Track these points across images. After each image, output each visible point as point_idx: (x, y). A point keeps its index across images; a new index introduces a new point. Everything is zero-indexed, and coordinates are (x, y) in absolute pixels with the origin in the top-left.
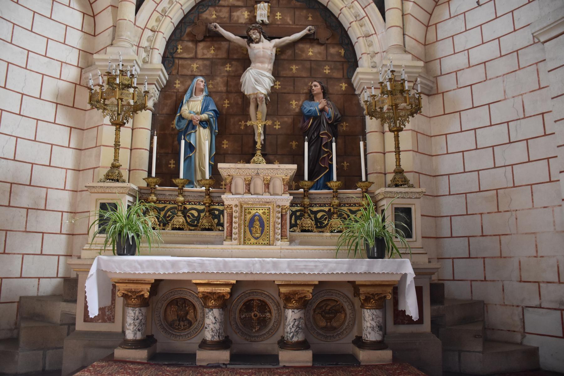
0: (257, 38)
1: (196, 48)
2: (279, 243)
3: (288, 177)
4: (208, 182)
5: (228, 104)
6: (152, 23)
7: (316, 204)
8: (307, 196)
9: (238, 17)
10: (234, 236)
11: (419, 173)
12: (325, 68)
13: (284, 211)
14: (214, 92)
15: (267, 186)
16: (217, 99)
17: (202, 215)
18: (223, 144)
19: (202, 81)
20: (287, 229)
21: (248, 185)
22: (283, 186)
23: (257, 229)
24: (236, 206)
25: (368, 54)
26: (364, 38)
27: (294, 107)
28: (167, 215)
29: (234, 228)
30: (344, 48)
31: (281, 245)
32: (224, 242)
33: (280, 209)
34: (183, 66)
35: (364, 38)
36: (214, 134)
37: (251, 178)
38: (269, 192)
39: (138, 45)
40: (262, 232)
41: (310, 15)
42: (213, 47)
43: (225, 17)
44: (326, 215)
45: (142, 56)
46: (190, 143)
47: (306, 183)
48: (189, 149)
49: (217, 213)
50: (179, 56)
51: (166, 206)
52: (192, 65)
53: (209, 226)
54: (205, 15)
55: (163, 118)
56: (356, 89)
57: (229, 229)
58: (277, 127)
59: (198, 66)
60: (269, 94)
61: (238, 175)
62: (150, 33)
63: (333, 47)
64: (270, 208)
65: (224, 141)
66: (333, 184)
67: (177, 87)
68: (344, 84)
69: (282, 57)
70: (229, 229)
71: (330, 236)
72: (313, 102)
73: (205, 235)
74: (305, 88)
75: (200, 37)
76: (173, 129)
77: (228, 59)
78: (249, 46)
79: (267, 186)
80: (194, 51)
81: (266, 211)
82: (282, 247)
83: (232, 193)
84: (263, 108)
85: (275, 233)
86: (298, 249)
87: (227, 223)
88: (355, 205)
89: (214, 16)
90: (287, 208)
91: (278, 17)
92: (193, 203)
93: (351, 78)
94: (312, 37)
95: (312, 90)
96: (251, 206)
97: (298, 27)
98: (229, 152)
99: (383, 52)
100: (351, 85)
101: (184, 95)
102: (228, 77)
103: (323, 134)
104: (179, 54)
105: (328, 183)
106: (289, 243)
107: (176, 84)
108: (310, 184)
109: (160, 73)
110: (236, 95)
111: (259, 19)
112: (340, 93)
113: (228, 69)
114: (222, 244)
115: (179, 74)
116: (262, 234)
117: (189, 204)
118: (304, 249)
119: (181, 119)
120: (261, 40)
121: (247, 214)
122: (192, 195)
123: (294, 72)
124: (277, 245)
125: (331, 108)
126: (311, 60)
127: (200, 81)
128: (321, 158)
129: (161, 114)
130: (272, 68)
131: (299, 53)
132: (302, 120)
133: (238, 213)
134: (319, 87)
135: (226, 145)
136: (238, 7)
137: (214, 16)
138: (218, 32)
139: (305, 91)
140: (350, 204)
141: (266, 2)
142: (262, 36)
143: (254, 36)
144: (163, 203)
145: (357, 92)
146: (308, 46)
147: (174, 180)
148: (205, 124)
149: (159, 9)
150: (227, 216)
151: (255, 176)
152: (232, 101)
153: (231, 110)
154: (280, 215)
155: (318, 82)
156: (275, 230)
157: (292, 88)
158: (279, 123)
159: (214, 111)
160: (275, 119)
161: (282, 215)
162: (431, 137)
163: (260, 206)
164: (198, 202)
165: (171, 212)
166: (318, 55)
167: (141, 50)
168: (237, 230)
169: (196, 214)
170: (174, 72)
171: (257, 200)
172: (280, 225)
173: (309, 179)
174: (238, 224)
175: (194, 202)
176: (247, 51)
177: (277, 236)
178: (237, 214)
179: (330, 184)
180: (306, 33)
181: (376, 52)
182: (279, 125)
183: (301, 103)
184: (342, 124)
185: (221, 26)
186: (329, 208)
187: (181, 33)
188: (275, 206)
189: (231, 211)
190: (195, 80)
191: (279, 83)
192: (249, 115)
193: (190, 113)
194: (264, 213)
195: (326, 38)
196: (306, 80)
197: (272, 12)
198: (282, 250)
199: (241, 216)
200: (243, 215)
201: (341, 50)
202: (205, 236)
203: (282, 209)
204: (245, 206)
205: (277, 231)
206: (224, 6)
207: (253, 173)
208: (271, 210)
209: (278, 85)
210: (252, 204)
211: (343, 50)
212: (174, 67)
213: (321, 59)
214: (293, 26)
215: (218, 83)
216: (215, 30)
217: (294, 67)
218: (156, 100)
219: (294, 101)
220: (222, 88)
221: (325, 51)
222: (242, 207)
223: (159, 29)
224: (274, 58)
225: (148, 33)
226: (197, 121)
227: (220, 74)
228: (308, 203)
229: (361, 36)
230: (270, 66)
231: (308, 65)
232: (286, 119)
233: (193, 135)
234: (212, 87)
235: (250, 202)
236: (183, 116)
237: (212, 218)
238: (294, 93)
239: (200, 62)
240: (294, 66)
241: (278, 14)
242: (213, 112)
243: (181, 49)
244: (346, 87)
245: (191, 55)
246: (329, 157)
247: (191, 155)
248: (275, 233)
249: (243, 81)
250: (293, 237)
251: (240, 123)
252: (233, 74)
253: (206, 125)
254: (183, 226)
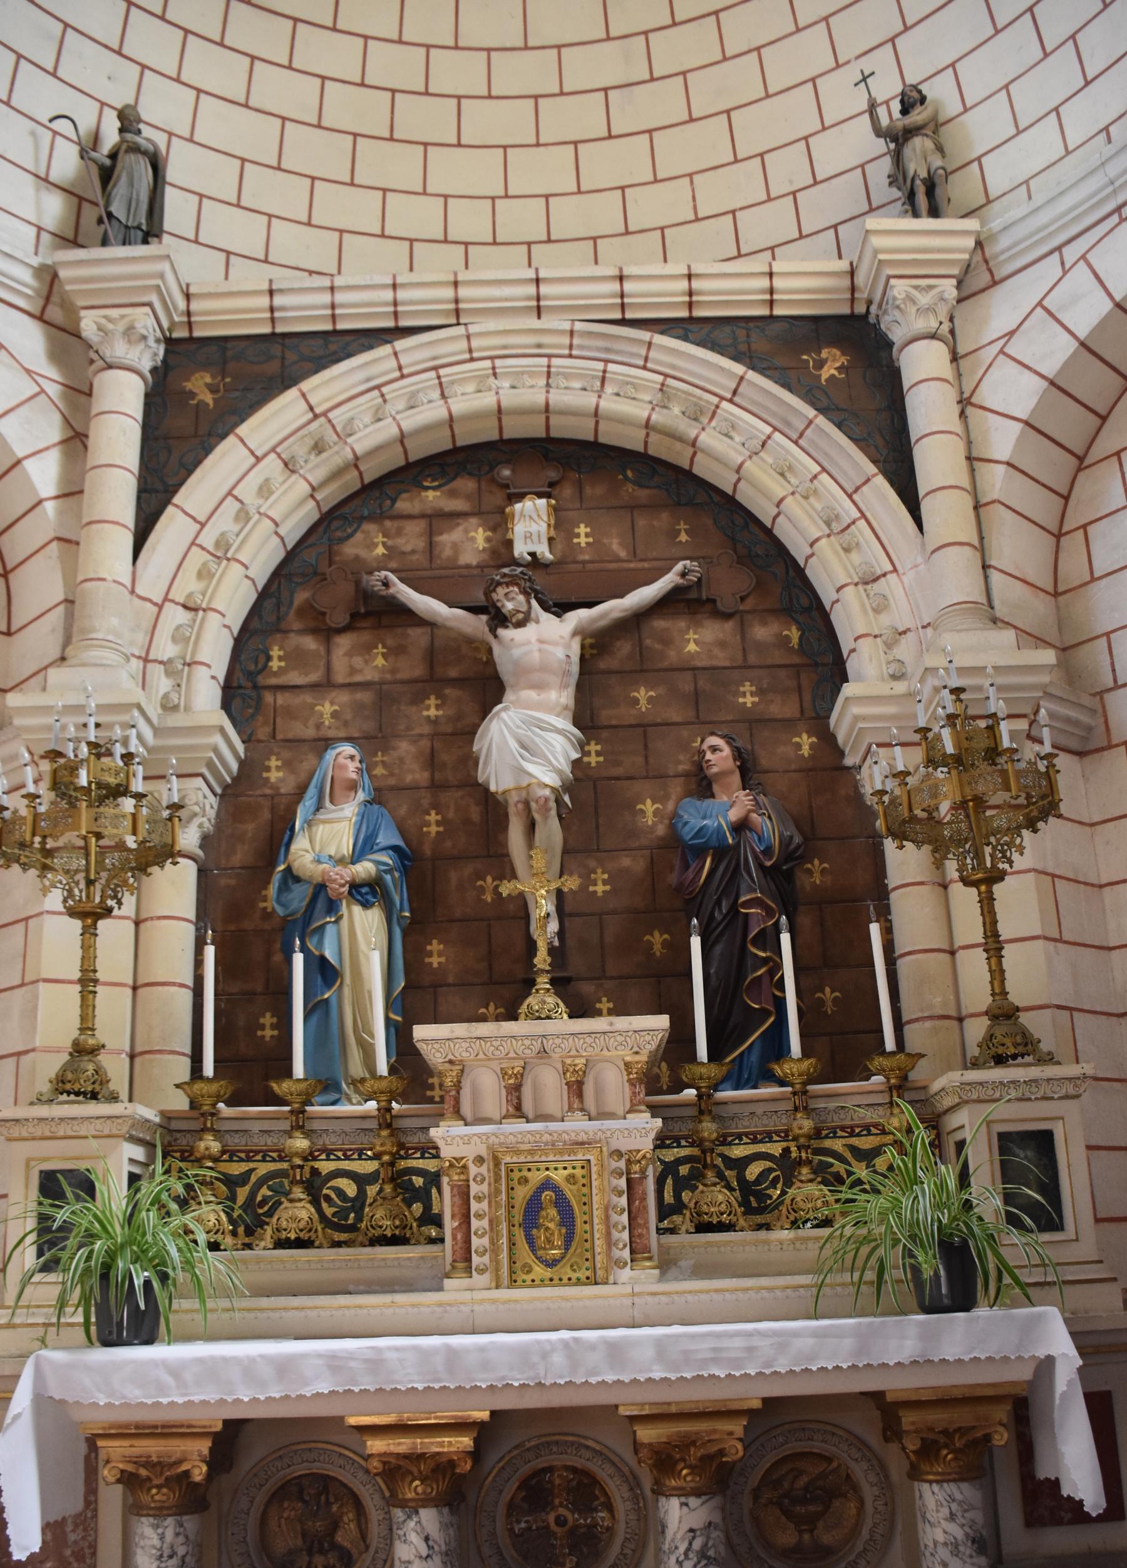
0: (519, 611)
1: (328, 652)
2: (626, 1274)
3: (643, 1058)
4: (384, 1085)
5: (438, 823)
6: (188, 585)
7: (739, 1136)
8: (710, 1112)
9: (455, 546)
10: (475, 1259)
11: (1071, 1009)
12: (742, 689)
13: (636, 1168)
14: (392, 788)
15: (576, 1089)
16: (403, 811)
17: (372, 1190)
18: (430, 954)
19: (352, 757)
20: (648, 1228)
21: (515, 1091)
22: (627, 1085)
23: (552, 1234)
24: (480, 1160)
25: (876, 636)
26: (860, 587)
27: (650, 823)
28: (259, 1198)
29: (476, 1234)
30: (797, 622)
31: (634, 1281)
32: (447, 1283)
33: (622, 1164)
34: (290, 713)
35: (860, 587)
36: (399, 924)
37: (524, 1068)
38: (582, 1110)
39: (143, 655)
40: (569, 1240)
41: (682, 526)
42: (380, 646)
43: (413, 552)
44: (775, 1170)
45: (157, 691)
46: (323, 959)
47: (703, 1070)
48: (319, 979)
49: (418, 1181)
50: (274, 681)
51: (254, 1170)
52: (318, 708)
53: (396, 1227)
54: (351, 549)
55: (233, 882)
56: (847, 752)
57: (459, 1237)
58: (600, 888)
59: (337, 708)
60: (567, 787)
61: (480, 1060)
62: (182, 616)
63: (764, 623)
64: (589, 1161)
65: (431, 944)
66: (791, 1069)
67: (273, 780)
68: (805, 736)
69: (603, 665)
70: (459, 1237)
71: (792, 1242)
72: (711, 800)
73: (384, 1259)
74: (682, 757)
75: (340, 618)
76: (267, 915)
78: (496, 636)
79: (576, 1089)
80: (322, 663)
81: (579, 1172)
82: (637, 1289)
83: (463, 1119)
84: (551, 831)
85: (610, 1243)
86: (690, 1292)
87: (453, 1217)
88: (869, 1131)
89: (380, 550)
90: (644, 1157)
91: (583, 540)
92: (340, 1154)
93: (829, 717)
94: (693, 595)
95: (705, 765)
96: (529, 1159)
97: (646, 565)
98: (451, 980)
99: (924, 627)
100: (827, 739)
101: (298, 802)
102: (433, 736)
103: (748, 904)
104: (275, 674)
105: (776, 1067)
106: (656, 1272)
107: (268, 769)
108: (715, 1071)
109: (218, 740)
110: (460, 793)
111: (521, 549)
112: (793, 767)
113: (433, 712)
114: (440, 1289)
115: (279, 736)
116: (567, 1249)
117: (328, 1159)
118: (708, 1292)
119: (290, 882)
120: (533, 615)
121: (515, 1184)
122: (337, 1129)
123: (644, 709)
124: (620, 1281)
125: (770, 818)
126: (694, 669)
128: (748, 980)
129: (225, 869)
130: (571, 703)
131: (657, 646)
132: (677, 863)
133: (486, 1183)
134: (727, 751)
135: (439, 956)
136: (454, 516)
137: (380, 550)
138: (393, 597)
139: (681, 768)
140: (852, 1128)
141: (540, 495)
142: (534, 603)
143: (509, 606)
144: (242, 1160)
145: (849, 761)
146: (682, 624)
147: (274, 1085)
148: (366, 894)
149: (208, 538)
150: (453, 1196)
151: (535, 1061)
152: (451, 815)
153: (448, 844)
154: (622, 1183)
155: (723, 737)
156: (608, 1234)
157: (640, 760)
158: (606, 876)
159: (395, 848)
160: (592, 863)
161: (629, 1181)
162: (1101, 886)
163: (558, 1158)
164: (357, 1149)
165: (269, 1188)
166: (716, 651)
167: (155, 671)
168: (485, 1241)
169: (351, 1189)
170: (263, 732)
171: (546, 1138)
172: (625, 1216)
173: (715, 1054)
174: (487, 1219)
175: (345, 1151)
176: (490, 651)
177: (616, 1253)
178: (485, 1188)
179: (782, 1070)
180: (673, 585)
181: (901, 629)
182: (605, 883)
183: (670, 806)
184: (809, 866)
185: (402, 580)
186: (784, 1144)
187: (279, 608)
188: (605, 1153)
189: (463, 1177)
190: (330, 755)
191: (599, 748)
192: (507, 855)
193: (319, 861)
194: (571, 1179)
195: (738, 597)
196: (685, 733)
197: (561, 524)
198: (636, 1300)
199: (498, 1192)
200: (503, 1188)
201: (790, 630)
202: (383, 1263)
203: (629, 1162)
204: (508, 1159)
205: (615, 1235)
206: (410, 517)
207: (527, 1051)
208: (594, 1169)
209: (593, 754)
210: (531, 1152)
211: (794, 629)
212: (260, 719)
213: (727, 664)
214: (632, 565)
215: (401, 760)
216: (384, 593)
217: (642, 695)
218: (207, 824)
219: (649, 802)
220: (417, 775)
221: (738, 637)
222: (497, 1162)
223: (210, 601)
224: (575, 668)
225: (175, 616)
226: (343, 886)
227: (408, 728)
228: (715, 1135)
229: (849, 581)
230: (566, 697)
231: (685, 684)
232: (626, 862)
233: (330, 930)
234: (384, 772)
235: (523, 1147)
236: (295, 872)
237: (403, 1200)
238: (646, 777)
239: (344, 697)
240: (643, 691)
241: (582, 529)
242: (391, 852)
243: (280, 658)
244: (812, 746)
245: (314, 677)
246: (772, 979)
247: (326, 996)
248: (610, 1243)
249: (480, 750)
250: (672, 1251)
251: (480, 883)
252: (449, 729)
253: (370, 898)
254: (312, 1233)
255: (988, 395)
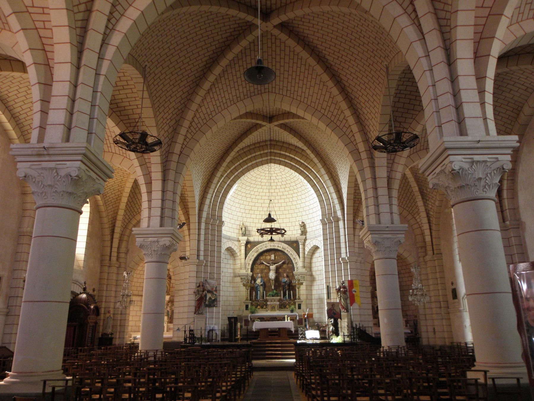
77: (265, 269)
84: (273, 282)
100: (293, 274)
127: (259, 275)
173: (283, 297)
197: (275, 256)
255: (306, 249)
